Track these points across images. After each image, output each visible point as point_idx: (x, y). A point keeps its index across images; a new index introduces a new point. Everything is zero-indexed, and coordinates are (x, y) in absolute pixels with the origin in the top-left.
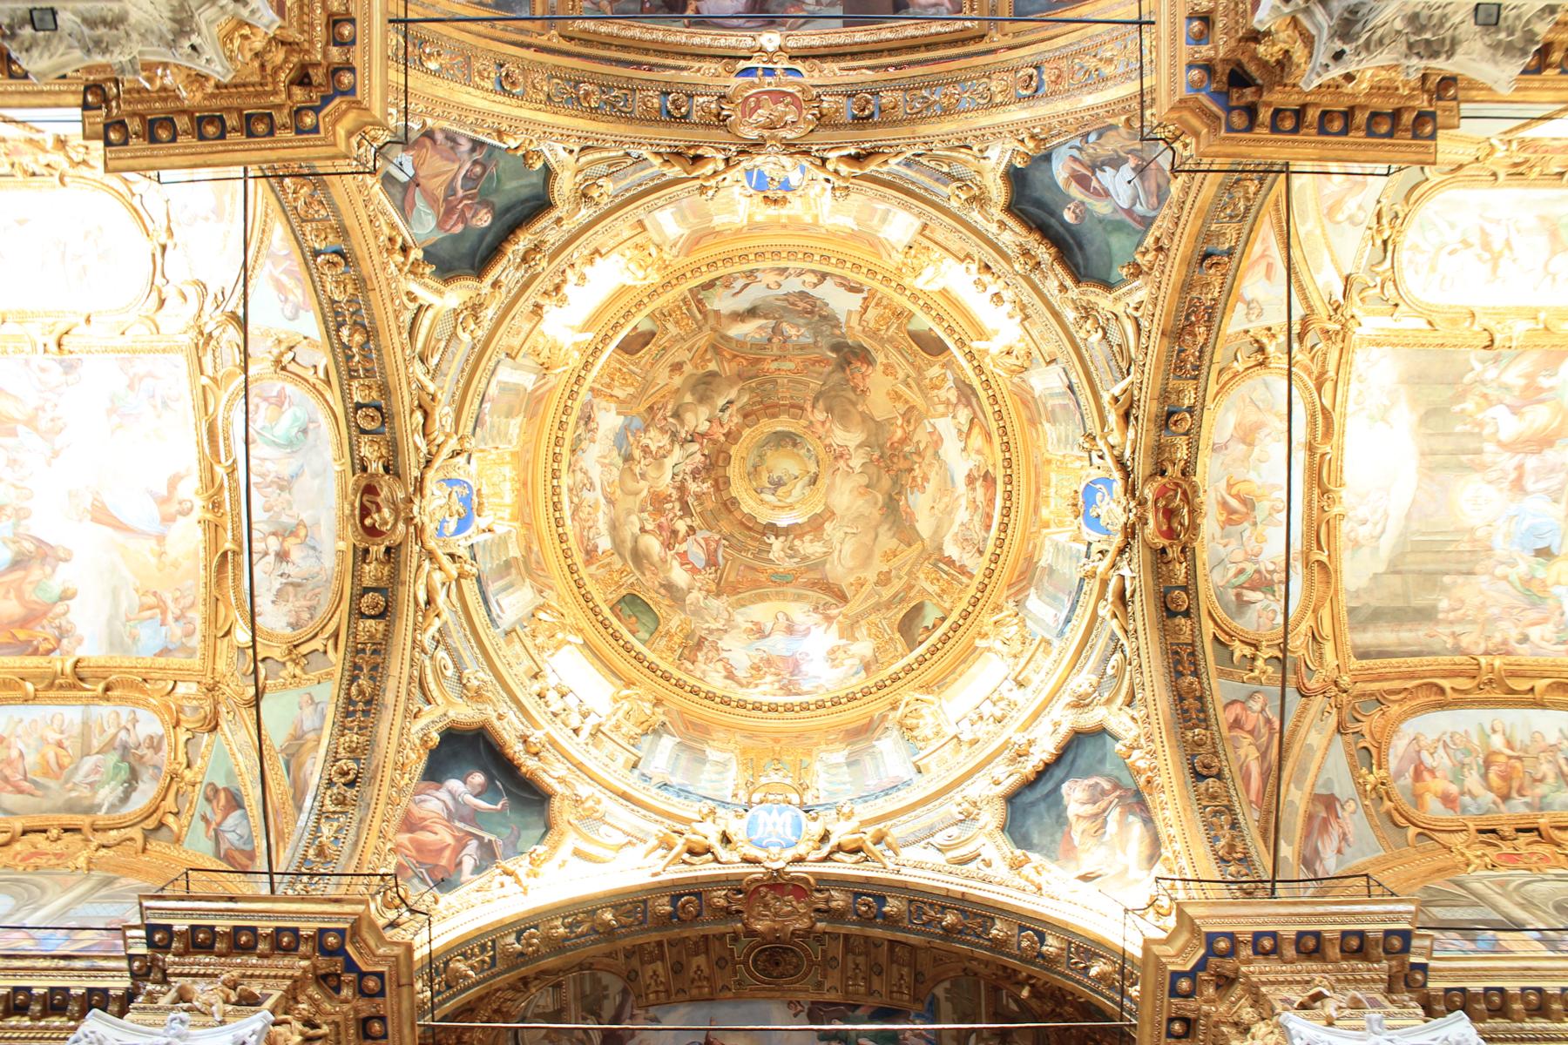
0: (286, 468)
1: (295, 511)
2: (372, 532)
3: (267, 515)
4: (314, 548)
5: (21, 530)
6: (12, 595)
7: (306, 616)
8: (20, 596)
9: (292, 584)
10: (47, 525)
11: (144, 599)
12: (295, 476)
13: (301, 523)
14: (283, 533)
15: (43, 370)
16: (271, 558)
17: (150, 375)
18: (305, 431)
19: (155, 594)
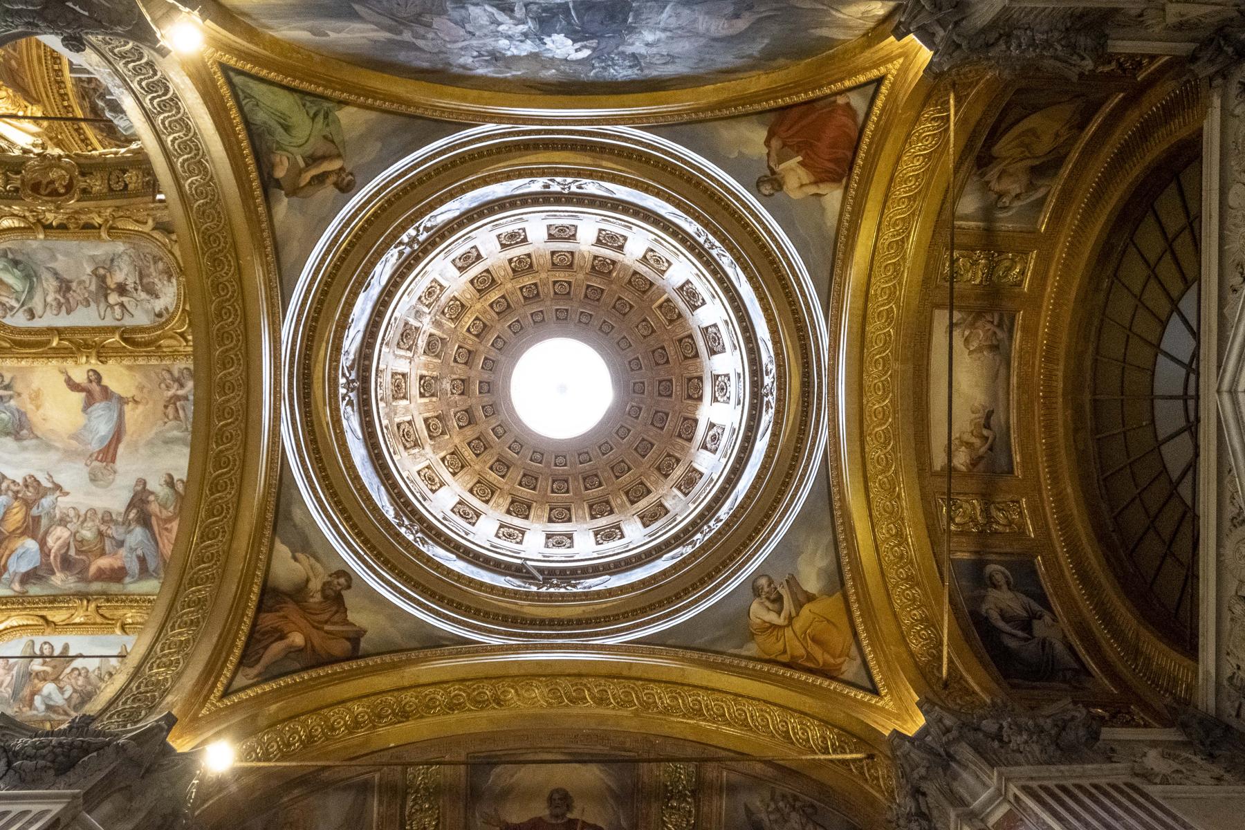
0: (51, 284)
2: (69, 188)
3: (92, 304)
4: (112, 260)
5: (120, 519)
6: (168, 526)
7: (160, 265)
8: (169, 520)
9: (141, 280)
10: (115, 500)
11: (171, 417)
12: (56, 275)
13: (94, 272)
14: (104, 290)
16: (124, 299)
19: (166, 407)
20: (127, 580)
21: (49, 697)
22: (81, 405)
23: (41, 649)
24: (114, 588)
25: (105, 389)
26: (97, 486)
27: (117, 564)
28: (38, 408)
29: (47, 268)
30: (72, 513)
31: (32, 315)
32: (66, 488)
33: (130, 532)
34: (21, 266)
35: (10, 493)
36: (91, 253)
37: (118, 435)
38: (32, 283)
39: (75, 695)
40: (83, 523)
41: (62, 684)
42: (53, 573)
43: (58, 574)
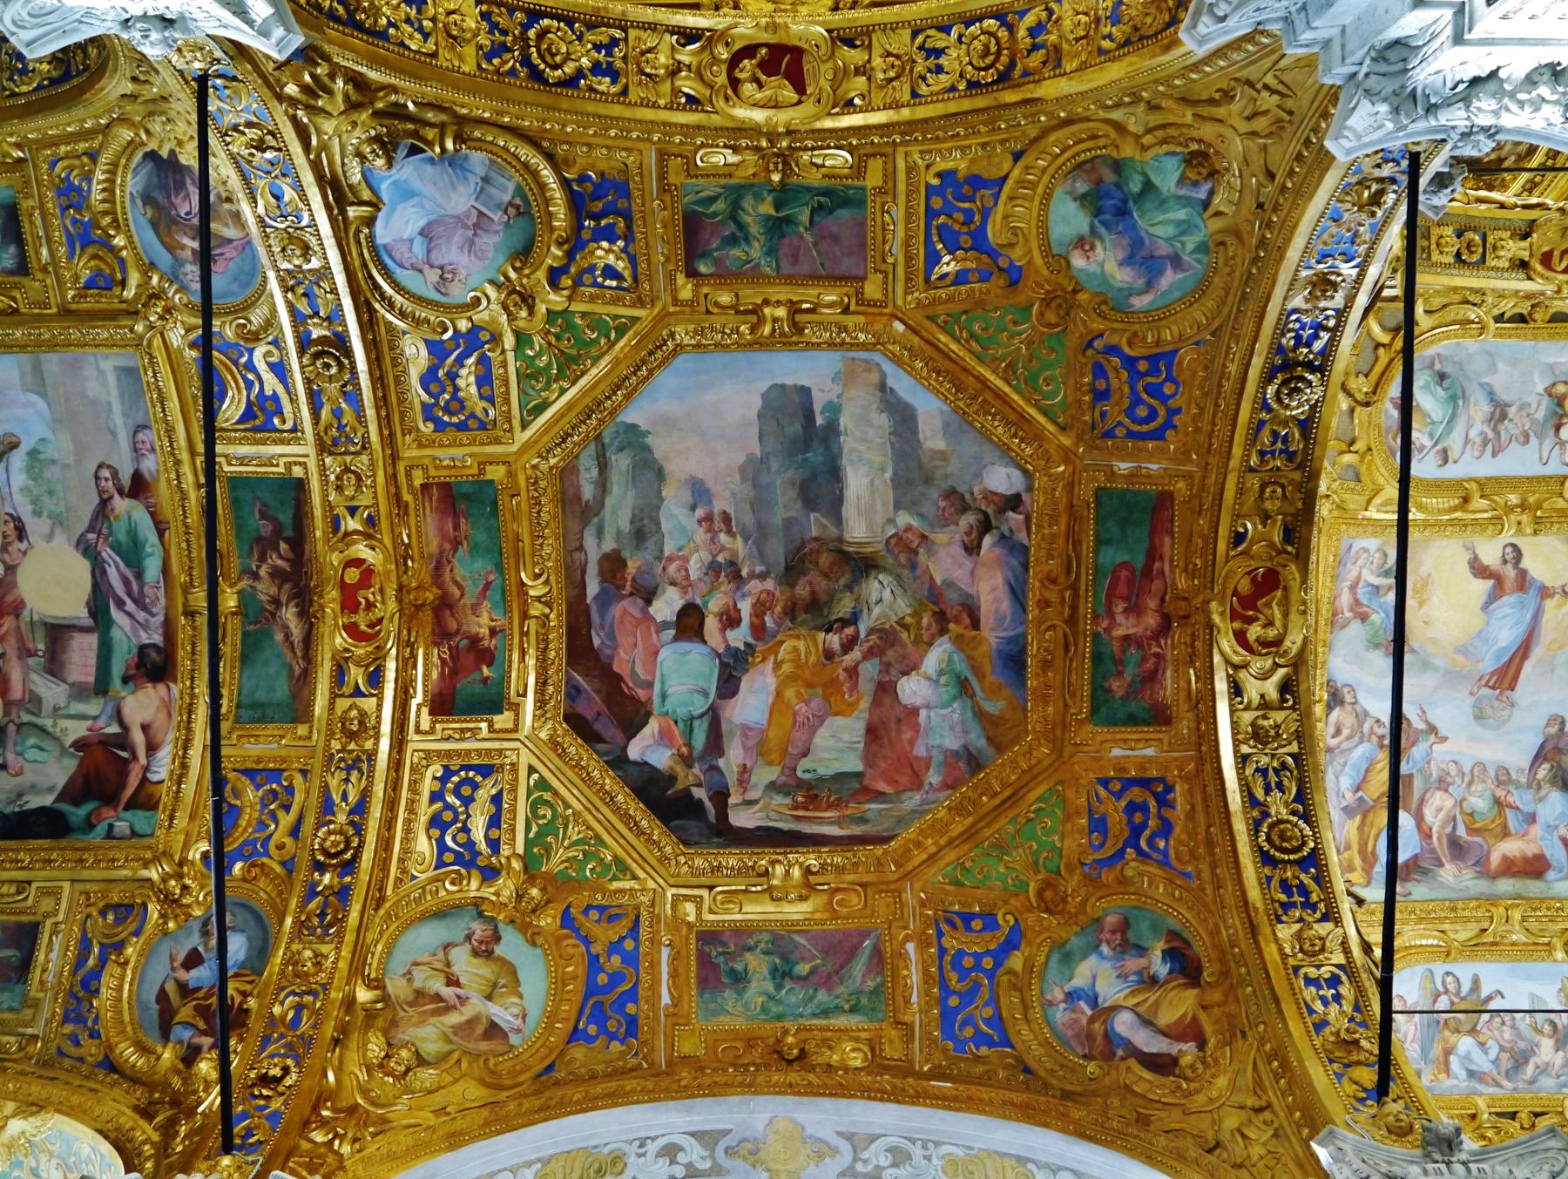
0: (1480, 408)
1: (1533, 400)
3: (1533, 441)
5: (1523, 780)
12: (1491, 396)
13: (1549, 392)
15: (1338, 732)
17: (1353, 588)
18: (1442, 377)
20: (1551, 875)
21: (1467, 1057)
22: (1483, 599)
23: (1444, 983)
24: (1533, 887)
25: (1523, 574)
26: (1482, 726)
27: (1531, 850)
28: (1421, 606)
29: (1481, 385)
30: (1453, 770)
31: (1445, 458)
32: (1443, 732)
33: (1540, 800)
34: (1446, 383)
35: (1374, 739)
36: (1552, 360)
37: (1524, 650)
38: (1455, 408)
39: (1505, 1056)
40: (1470, 784)
41: (1482, 1039)
42: (1441, 865)
43: (1448, 866)
